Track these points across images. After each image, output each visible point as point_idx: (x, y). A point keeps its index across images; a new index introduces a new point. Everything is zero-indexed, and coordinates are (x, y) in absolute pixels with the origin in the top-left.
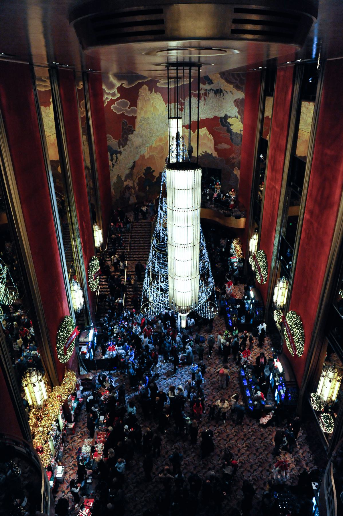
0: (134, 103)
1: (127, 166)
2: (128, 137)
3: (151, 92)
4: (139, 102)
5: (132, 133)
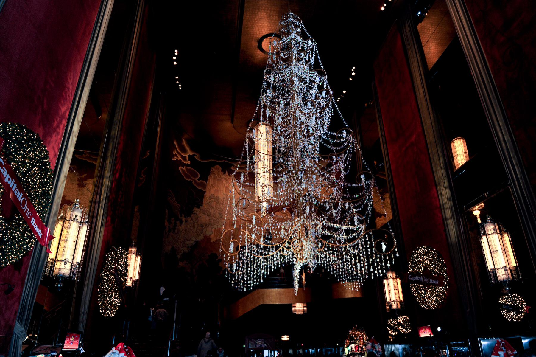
0: (205, 177)
1: (187, 243)
2: (193, 209)
3: (225, 173)
4: (211, 180)
5: (199, 208)
